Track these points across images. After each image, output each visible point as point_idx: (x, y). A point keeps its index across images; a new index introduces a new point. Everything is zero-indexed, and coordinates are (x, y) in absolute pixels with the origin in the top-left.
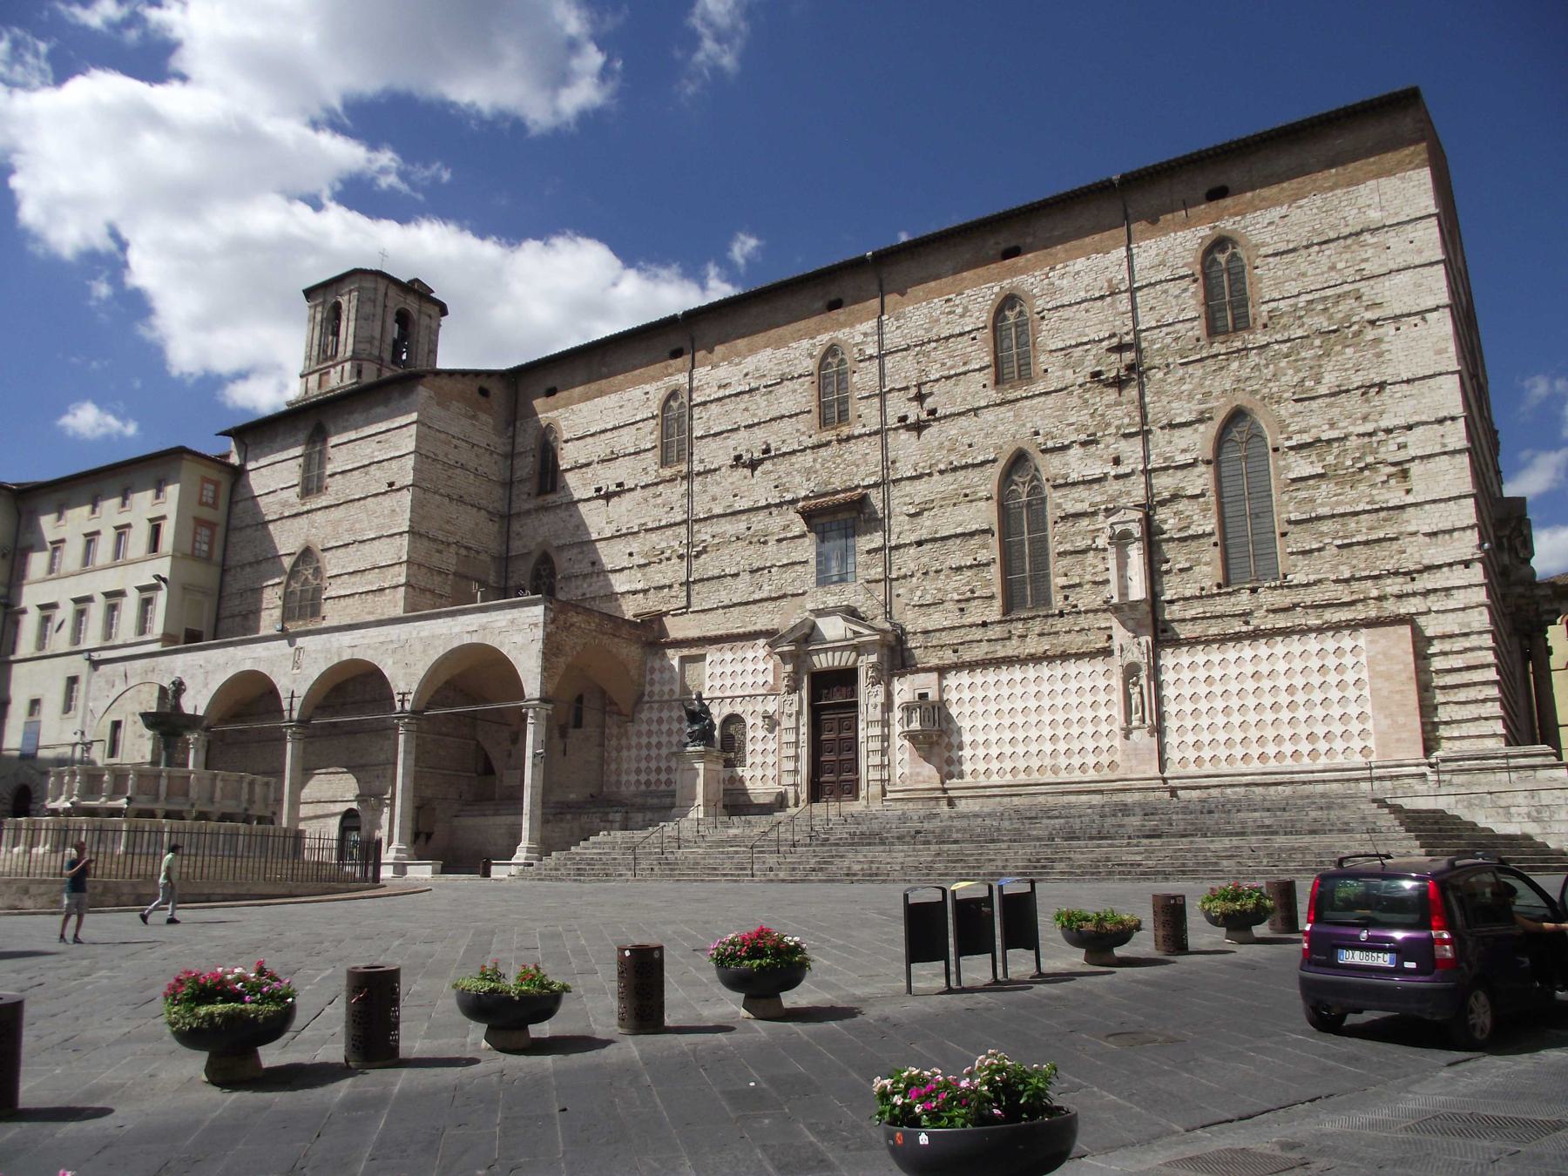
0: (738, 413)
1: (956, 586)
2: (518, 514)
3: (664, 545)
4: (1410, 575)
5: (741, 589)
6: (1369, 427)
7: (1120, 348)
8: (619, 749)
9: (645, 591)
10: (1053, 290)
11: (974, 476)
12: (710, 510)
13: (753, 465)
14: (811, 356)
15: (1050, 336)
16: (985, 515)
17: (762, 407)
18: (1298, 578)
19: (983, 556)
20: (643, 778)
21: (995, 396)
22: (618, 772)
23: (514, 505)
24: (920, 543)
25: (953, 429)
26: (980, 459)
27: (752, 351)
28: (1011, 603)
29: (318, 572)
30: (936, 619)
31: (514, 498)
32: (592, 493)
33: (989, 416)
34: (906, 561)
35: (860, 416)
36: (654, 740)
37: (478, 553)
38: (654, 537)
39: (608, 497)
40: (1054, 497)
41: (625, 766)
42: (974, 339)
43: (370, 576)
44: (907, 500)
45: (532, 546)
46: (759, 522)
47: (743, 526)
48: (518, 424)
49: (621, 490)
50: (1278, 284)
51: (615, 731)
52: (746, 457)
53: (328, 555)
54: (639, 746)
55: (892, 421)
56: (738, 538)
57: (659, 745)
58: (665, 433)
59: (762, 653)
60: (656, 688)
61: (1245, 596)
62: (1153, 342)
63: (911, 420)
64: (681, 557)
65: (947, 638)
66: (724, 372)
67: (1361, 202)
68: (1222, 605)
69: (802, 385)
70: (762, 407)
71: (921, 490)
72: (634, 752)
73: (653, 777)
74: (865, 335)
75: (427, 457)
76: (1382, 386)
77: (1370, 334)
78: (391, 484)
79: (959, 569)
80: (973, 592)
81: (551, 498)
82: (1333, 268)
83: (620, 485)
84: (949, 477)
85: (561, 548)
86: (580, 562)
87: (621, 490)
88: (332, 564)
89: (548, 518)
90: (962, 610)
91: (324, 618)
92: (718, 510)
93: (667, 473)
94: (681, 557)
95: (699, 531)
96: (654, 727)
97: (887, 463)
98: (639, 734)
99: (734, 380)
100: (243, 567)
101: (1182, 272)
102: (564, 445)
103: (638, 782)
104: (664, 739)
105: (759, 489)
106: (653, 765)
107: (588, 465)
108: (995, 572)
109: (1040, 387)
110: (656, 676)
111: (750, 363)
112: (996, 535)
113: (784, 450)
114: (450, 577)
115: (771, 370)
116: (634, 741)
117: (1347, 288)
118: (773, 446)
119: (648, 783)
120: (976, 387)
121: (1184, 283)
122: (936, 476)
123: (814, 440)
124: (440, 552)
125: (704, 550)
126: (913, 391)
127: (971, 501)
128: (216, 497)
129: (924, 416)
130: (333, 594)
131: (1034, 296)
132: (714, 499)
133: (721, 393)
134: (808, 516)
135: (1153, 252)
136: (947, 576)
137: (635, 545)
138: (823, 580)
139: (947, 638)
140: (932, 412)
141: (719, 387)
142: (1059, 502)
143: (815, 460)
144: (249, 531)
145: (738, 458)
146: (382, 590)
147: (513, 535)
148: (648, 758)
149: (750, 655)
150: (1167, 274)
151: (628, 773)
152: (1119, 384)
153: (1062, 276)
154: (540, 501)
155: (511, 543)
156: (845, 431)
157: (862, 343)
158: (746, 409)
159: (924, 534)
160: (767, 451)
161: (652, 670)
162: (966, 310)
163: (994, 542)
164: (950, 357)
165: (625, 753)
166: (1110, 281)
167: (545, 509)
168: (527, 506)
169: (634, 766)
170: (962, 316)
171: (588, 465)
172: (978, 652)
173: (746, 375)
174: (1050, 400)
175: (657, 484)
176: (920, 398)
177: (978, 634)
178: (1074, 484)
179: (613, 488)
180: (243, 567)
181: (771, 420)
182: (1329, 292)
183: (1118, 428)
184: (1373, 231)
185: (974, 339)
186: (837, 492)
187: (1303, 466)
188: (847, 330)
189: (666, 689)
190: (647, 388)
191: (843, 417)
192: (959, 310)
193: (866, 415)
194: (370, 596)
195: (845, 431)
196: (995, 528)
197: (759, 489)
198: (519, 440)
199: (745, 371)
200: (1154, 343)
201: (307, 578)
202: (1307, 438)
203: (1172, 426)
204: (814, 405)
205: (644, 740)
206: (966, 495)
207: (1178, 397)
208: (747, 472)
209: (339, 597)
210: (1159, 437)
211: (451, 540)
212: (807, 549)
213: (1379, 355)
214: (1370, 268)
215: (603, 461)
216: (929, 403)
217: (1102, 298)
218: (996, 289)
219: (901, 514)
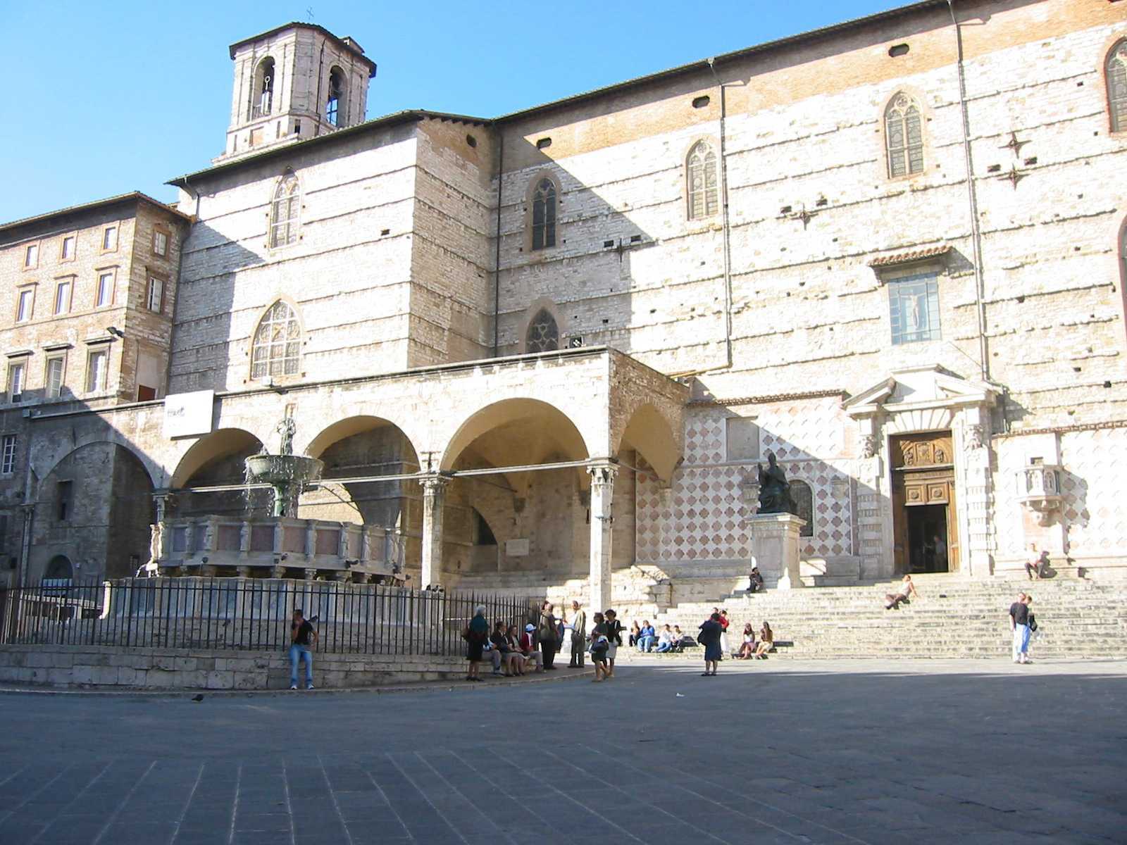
0: (781, 162)
2: (508, 270)
5: (799, 346)
8: (655, 517)
12: (752, 265)
13: (806, 217)
14: (874, 103)
17: (812, 156)
19: (1103, 313)
20: (685, 547)
22: (655, 543)
23: (502, 261)
25: (1056, 179)
30: (1047, 379)
31: (501, 253)
34: (1004, 317)
35: (938, 166)
36: (698, 507)
37: (469, 309)
41: (662, 535)
42: (1080, 84)
44: (1004, 254)
45: (527, 302)
46: (816, 277)
48: (505, 177)
51: (648, 497)
52: (796, 209)
54: (680, 515)
55: (981, 170)
56: (789, 294)
57: (704, 513)
60: (698, 453)
63: (1006, 168)
65: (1058, 398)
70: (812, 156)
71: (1020, 244)
72: (673, 521)
73: (698, 547)
74: (942, 81)
75: (425, 204)
78: (386, 232)
80: (1090, 351)
81: (548, 253)
84: (1055, 230)
85: (563, 306)
86: (589, 320)
88: (310, 317)
89: (543, 274)
90: (1078, 370)
91: (304, 375)
95: (739, 288)
96: (698, 494)
98: (679, 502)
100: (198, 322)
102: (562, 198)
103: (680, 553)
104: (710, 507)
106: (698, 534)
110: (698, 439)
112: (1119, 290)
114: (446, 333)
116: (672, 508)
119: (692, 553)
122: (1039, 227)
123: (883, 191)
124: (437, 305)
126: (1007, 139)
127: (1085, 255)
128: (167, 249)
129: (1020, 165)
132: (757, 253)
133: (761, 142)
136: (1058, 334)
138: (898, 338)
139: (1058, 398)
140: (1033, 161)
143: (883, 212)
144: (203, 283)
147: (501, 292)
148: (691, 527)
151: (666, 542)
154: (536, 256)
155: (500, 299)
156: (921, 181)
160: (823, 202)
161: (692, 433)
162: (1069, 54)
164: (1051, 103)
165: (661, 522)
167: (542, 264)
168: (520, 262)
169: (673, 534)
176: (1016, 145)
180: (198, 322)
185: (1080, 84)
189: (711, 453)
190: (665, 137)
191: (915, 167)
194: (363, 351)
195: (921, 181)
196: (1118, 283)
198: (505, 193)
204: (880, 154)
205: (685, 508)
206: (1078, 249)
211: (447, 294)
216: (1026, 152)
219: (996, 268)
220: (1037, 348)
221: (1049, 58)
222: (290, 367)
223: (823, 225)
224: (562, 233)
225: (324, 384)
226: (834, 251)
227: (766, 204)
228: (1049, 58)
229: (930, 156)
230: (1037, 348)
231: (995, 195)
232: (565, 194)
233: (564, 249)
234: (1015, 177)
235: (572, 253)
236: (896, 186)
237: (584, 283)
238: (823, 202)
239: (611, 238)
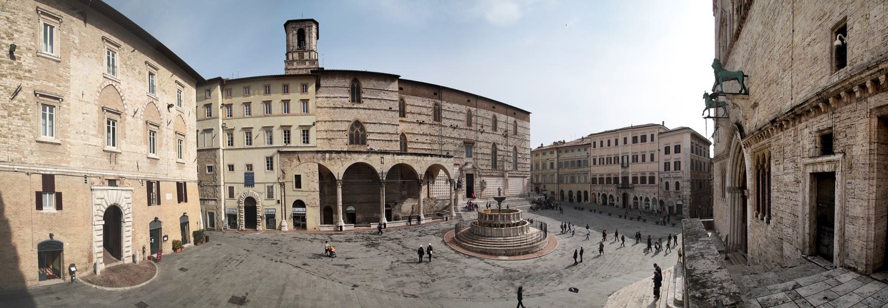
1: (486, 162)
3: (435, 140)
4: (526, 172)
7: (506, 131)
9: (431, 150)
11: (489, 145)
15: (501, 125)
16: (489, 151)
17: (456, 116)
18: (519, 170)
19: (490, 158)
21: (491, 131)
24: (481, 154)
25: (487, 135)
27: (454, 103)
28: (492, 167)
29: (363, 129)
30: (484, 168)
32: (416, 121)
33: (491, 135)
34: (480, 156)
38: (433, 137)
39: (420, 123)
40: (498, 151)
43: (386, 135)
46: (456, 141)
47: (452, 141)
49: (422, 123)
52: (453, 126)
53: (368, 125)
55: (478, 129)
58: (439, 114)
59: (458, 169)
64: (439, 144)
66: (449, 105)
68: (513, 172)
70: (456, 116)
71: (482, 144)
79: (486, 160)
81: (404, 119)
83: (423, 121)
87: (422, 123)
91: (368, 145)
92: (448, 136)
93: (436, 123)
94: (439, 144)
97: (478, 137)
105: (455, 134)
107: (414, 113)
108: (491, 161)
109: (497, 133)
111: (455, 105)
113: (460, 127)
118: (459, 126)
120: (488, 129)
125: (444, 144)
130: (371, 138)
132: (447, 133)
133: (448, 109)
134: (465, 143)
137: (428, 138)
142: (499, 153)
145: (451, 125)
146: (391, 141)
149: (456, 169)
152: (505, 137)
156: (471, 128)
159: (482, 152)
160: (457, 126)
171: (414, 113)
172: (488, 174)
174: (498, 136)
175: (433, 125)
176: (482, 127)
177: (489, 171)
178: (500, 150)
179: (421, 122)
186: (469, 139)
193: (474, 127)
194: (387, 142)
197: (455, 134)
200: (509, 132)
201: (357, 131)
203: (510, 146)
204: (466, 120)
208: (453, 129)
209: (374, 140)
210: (509, 147)
212: (464, 149)
215: (419, 114)
220: (483, 162)
222: (364, 142)
223: (457, 131)
224: (407, 115)
225: (392, 153)
226: (458, 137)
227: (448, 125)
229: (473, 125)
230: (483, 162)
231: (479, 134)
232: (408, 105)
233: (407, 118)
234: (482, 132)
235: (410, 121)
237: (412, 129)
238: (457, 126)
239: (418, 119)
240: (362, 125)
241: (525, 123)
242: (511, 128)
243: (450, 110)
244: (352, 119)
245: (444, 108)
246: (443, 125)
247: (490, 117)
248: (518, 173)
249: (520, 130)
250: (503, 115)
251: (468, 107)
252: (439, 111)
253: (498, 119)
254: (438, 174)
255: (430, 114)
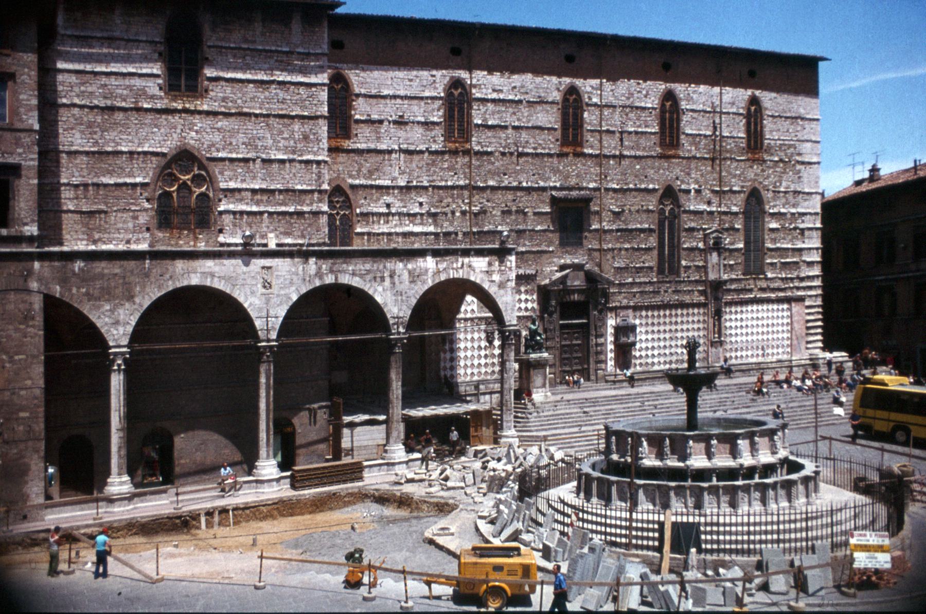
4: (802, 279)
6: (793, 211)
10: (689, 99)
14: (558, 89)
15: (689, 126)
18: (770, 275)
26: (651, 186)
28: (661, 271)
50: (771, 131)
61: (751, 282)
62: (727, 144)
67: (799, 103)
69: (552, 108)
70: (525, 117)
74: (592, 87)
76: (799, 192)
77: (798, 167)
82: (788, 131)
99: (505, 89)
101: (741, 111)
111: (517, 79)
115: (531, 90)
117: (792, 143)
121: (741, 117)
131: (681, 99)
133: (495, 96)
135: (730, 95)
141: (494, 90)
150: (734, 110)
153: (694, 92)
156: (579, 149)
157: (591, 93)
158: (514, 113)
162: (647, 92)
163: (655, 235)
166: (713, 103)
170: (646, 96)
173: (515, 87)
181: (533, 128)
182: (787, 142)
183: (711, 185)
184: (803, 119)
187: (774, 225)
188: (582, 80)
192: (644, 92)
195: (579, 149)
199: (513, 85)
202: (775, 210)
207: (735, 176)
213: (799, 177)
214: (800, 137)
217: (709, 112)
218: (663, 87)
221: (639, 92)
228: (639, 92)
236: (565, 150)
240: (202, 167)
241: (801, 105)
242: (736, 130)
243: (502, 96)
244: (167, 146)
245: (478, 95)
246: (477, 148)
247: (652, 102)
248: (764, 284)
249: (773, 132)
250: (702, 88)
251: (567, 80)
252: (461, 103)
253: (684, 105)
254: (458, 311)
255: (435, 119)
